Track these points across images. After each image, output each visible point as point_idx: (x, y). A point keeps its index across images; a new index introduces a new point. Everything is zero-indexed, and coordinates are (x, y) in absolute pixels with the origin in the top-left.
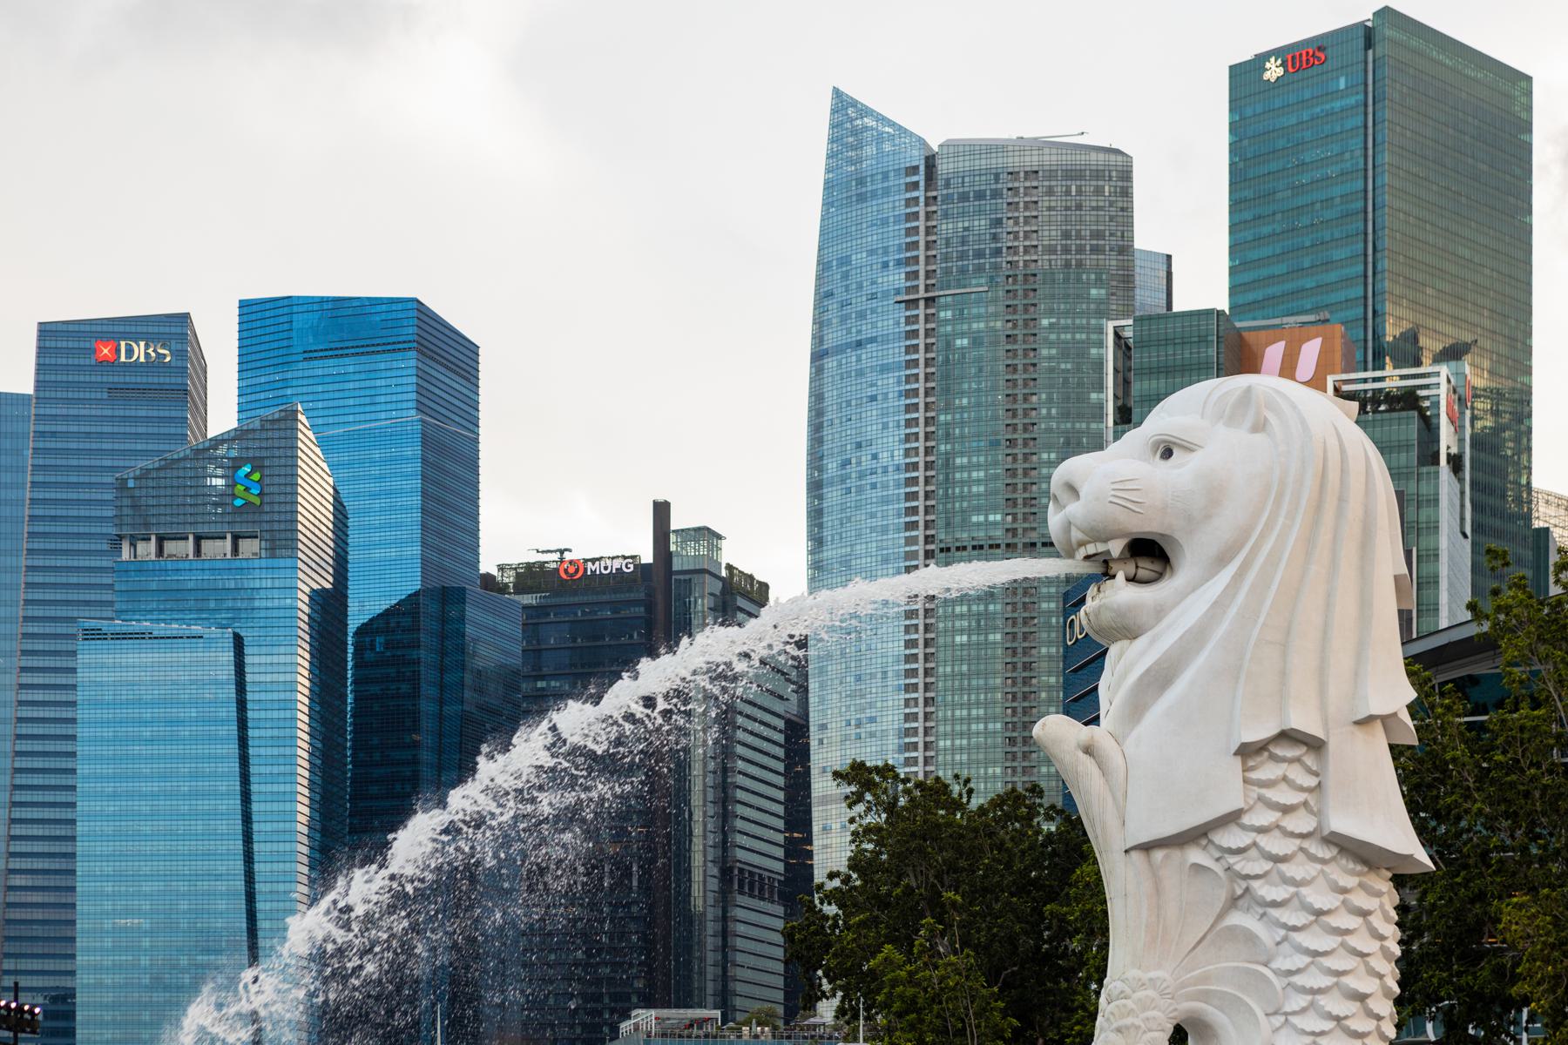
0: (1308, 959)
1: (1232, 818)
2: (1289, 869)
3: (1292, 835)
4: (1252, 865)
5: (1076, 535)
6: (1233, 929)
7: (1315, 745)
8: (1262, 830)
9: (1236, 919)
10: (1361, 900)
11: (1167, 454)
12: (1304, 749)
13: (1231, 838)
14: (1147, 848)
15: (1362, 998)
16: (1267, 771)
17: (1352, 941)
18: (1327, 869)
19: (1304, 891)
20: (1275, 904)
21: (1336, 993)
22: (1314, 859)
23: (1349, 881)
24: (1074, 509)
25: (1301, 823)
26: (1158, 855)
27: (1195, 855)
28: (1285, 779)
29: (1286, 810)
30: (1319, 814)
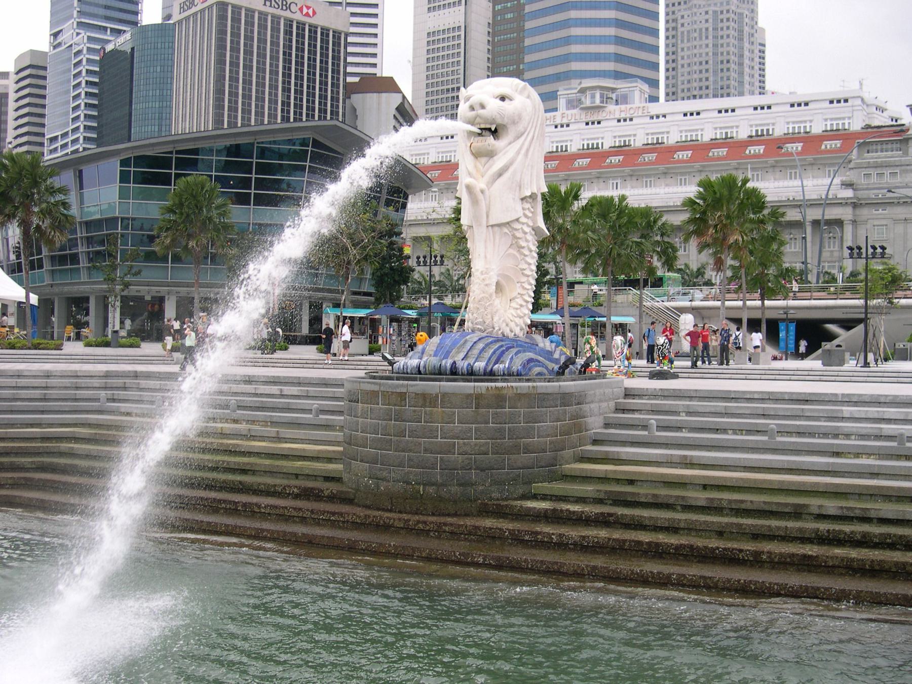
1: (517, 220)
3: (528, 226)
5: (478, 120)
6: (509, 255)
8: (523, 224)
9: (511, 251)
11: (503, 99)
13: (516, 226)
14: (492, 226)
16: (527, 206)
20: (523, 248)
22: (531, 234)
24: (481, 112)
26: (496, 228)
27: (506, 230)
30: (535, 221)
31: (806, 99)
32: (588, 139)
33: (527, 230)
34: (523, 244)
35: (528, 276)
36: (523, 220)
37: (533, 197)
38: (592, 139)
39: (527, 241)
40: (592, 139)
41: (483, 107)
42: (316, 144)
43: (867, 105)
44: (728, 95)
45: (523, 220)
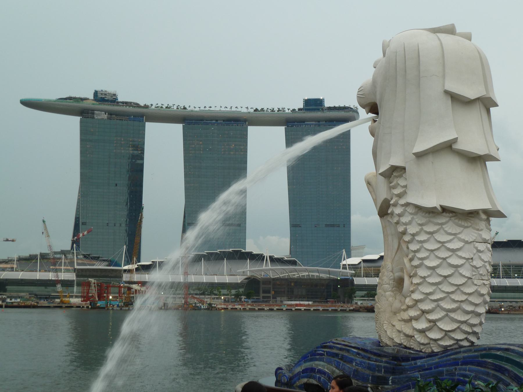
0: (413, 254)
2: (404, 220)
4: (395, 220)
7: (404, 169)
10: (430, 228)
12: (403, 171)
15: (433, 268)
17: (428, 246)
18: (415, 217)
19: (408, 227)
21: (423, 267)
22: (411, 214)
23: (423, 221)
25: (402, 201)
28: (399, 184)
29: (400, 196)
34: (401, 229)
35: (416, 267)
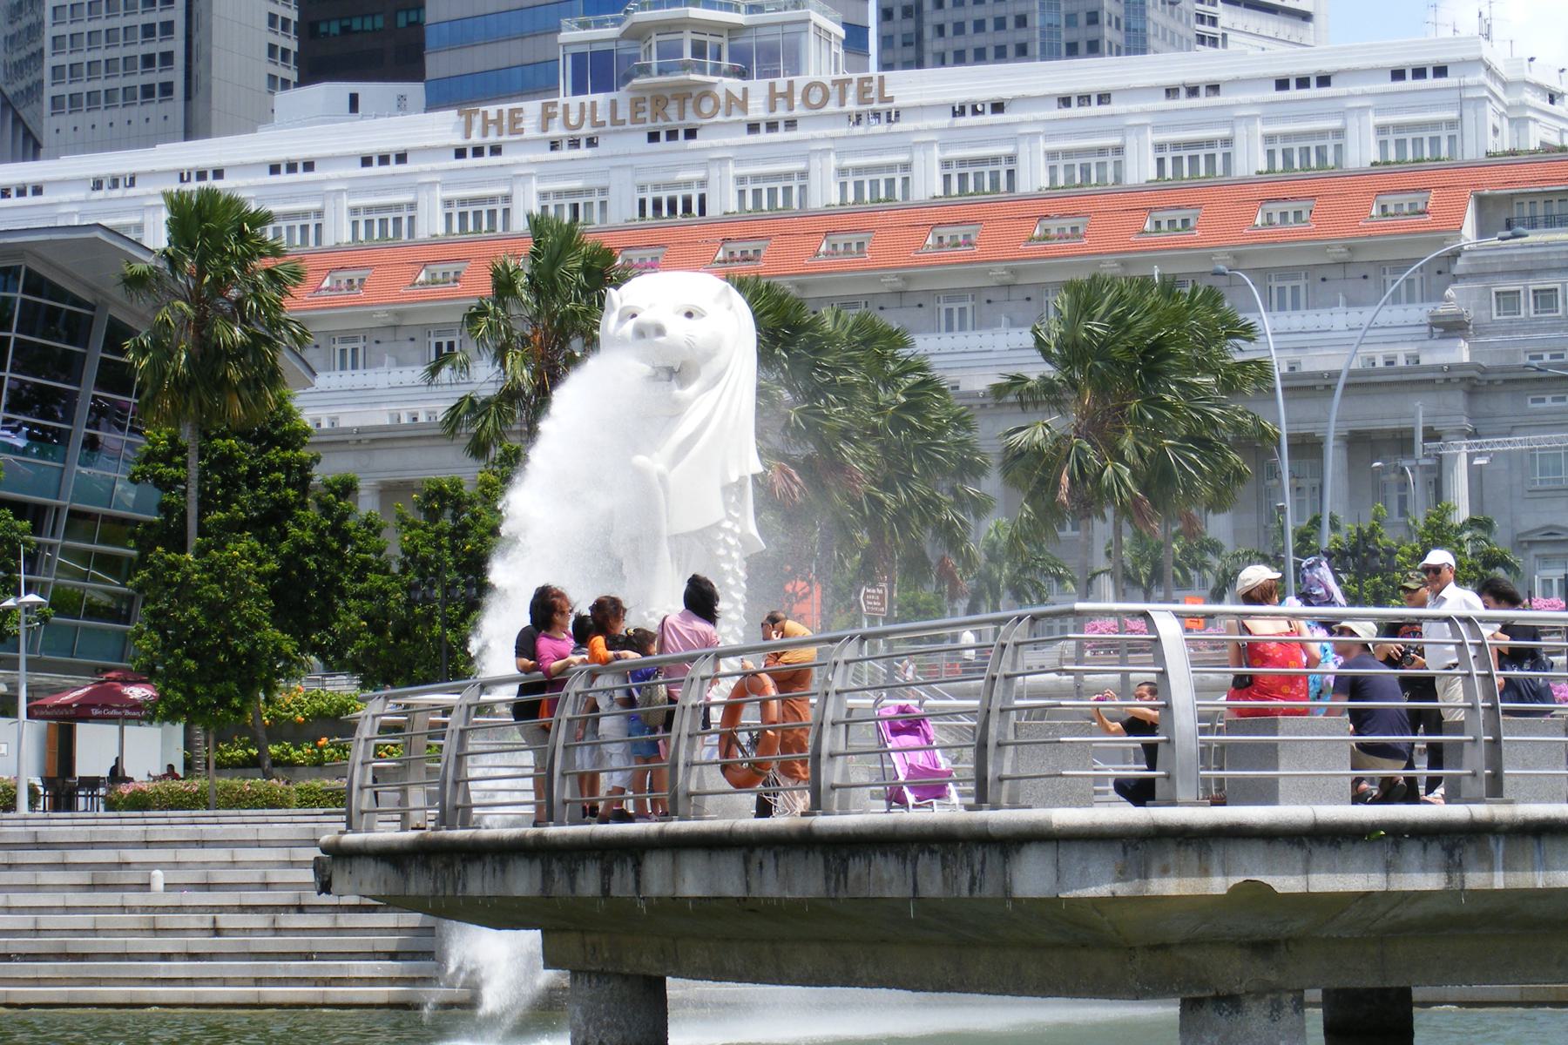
1: (717, 526)
3: (734, 535)
11: (689, 315)
31: (1326, 67)
32: (657, 187)
33: (732, 541)
36: (727, 525)
37: (740, 484)
38: (668, 186)
39: (731, 561)
40: (668, 186)
41: (660, 331)
42: (36, 284)
43: (1506, 84)
44: (1094, 48)
45: (727, 525)
